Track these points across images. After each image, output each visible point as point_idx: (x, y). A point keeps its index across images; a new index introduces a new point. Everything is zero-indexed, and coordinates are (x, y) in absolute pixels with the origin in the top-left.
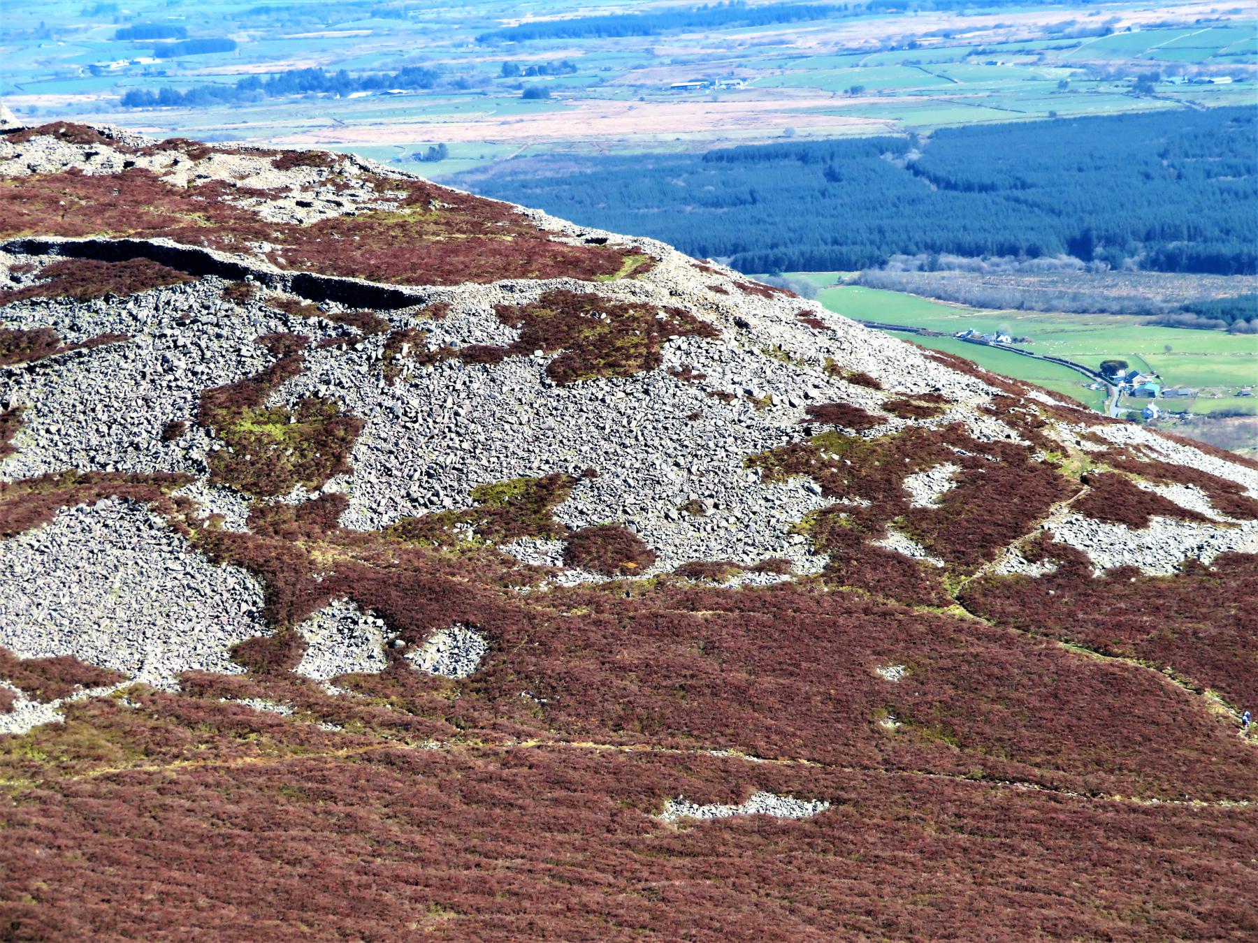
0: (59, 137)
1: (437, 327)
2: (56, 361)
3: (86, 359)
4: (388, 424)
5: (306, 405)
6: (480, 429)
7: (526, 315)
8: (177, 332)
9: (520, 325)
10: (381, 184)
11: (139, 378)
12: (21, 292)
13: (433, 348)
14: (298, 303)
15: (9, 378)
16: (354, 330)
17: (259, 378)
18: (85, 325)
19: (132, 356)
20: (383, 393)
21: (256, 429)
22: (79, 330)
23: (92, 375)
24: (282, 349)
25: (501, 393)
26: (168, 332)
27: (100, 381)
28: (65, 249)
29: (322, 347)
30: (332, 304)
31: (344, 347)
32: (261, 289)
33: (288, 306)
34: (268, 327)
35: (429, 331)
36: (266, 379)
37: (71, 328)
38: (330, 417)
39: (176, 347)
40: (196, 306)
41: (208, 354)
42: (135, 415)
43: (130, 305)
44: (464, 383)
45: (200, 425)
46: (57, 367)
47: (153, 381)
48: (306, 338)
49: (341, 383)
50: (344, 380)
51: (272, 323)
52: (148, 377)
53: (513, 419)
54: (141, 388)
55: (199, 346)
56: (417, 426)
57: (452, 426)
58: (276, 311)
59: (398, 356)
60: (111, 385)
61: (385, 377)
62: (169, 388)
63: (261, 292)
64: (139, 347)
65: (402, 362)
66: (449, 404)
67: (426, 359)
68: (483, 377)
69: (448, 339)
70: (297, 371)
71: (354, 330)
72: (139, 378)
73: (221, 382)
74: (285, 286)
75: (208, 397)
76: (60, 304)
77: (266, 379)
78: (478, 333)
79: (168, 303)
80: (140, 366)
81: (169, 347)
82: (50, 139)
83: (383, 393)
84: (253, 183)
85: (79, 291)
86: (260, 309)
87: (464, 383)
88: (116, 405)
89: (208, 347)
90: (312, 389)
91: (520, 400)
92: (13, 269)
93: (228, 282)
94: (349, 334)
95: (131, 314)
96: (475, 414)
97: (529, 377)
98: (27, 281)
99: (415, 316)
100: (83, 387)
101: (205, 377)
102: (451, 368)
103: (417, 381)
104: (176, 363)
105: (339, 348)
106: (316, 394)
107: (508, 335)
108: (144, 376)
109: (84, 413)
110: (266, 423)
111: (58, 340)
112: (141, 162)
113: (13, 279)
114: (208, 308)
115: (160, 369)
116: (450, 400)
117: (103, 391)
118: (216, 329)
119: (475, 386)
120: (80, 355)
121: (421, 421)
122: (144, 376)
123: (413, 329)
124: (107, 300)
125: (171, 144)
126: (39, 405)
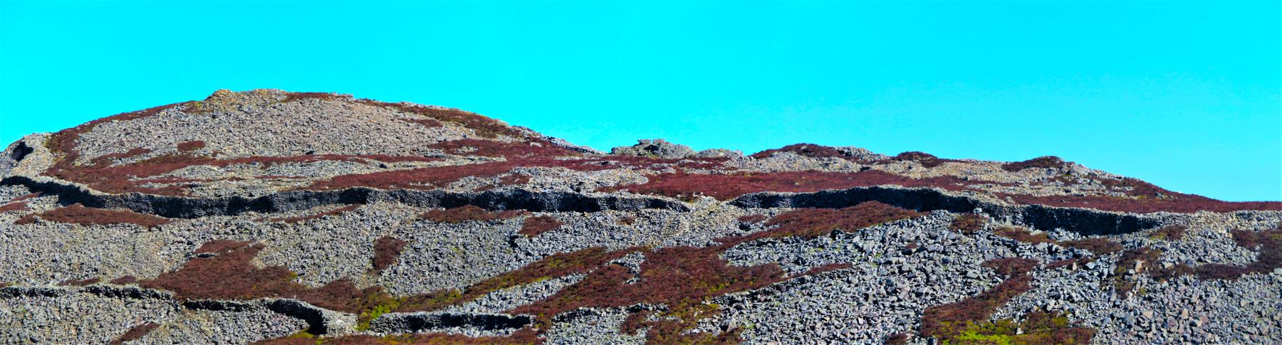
0: (800, 153)
1: (1172, 246)
2: (778, 288)
3: (809, 284)
4: (1120, 334)
5: (1033, 319)
6: (1217, 339)
7: (1264, 238)
8: (902, 260)
9: (1258, 248)
10: (1108, 183)
11: (861, 300)
12: (750, 237)
13: (1167, 265)
14: (1028, 233)
15: (730, 304)
16: (1085, 252)
17: (985, 296)
18: (810, 259)
19: (855, 281)
20: (1114, 306)
21: (981, 338)
22: (804, 263)
23: (814, 299)
24: (1010, 269)
25: (1240, 306)
26: (894, 260)
27: (822, 302)
28: (798, 201)
29: (1052, 267)
30: (1063, 233)
31: (1075, 267)
32: (990, 221)
33: (1017, 235)
34: (996, 254)
35: (1164, 250)
36: (994, 296)
37: (796, 262)
38: (1059, 328)
39: (901, 272)
40: (922, 236)
41: (934, 277)
42: (855, 331)
43: (857, 239)
44: (1201, 297)
45: (922, 336)
46: (779, 294)
47: (875, 302)
48: (1035, 262)
49: (1071, 297)
50: (1074, 295)
51: (1000, 250)
52: (871, 299)
53: (1254, 330)
54: (863, 308)
55: (925, 271)
56: (1150, 335)
57: (1188, 336)
58: (1005, 238)
59: (1131, 271)
60: (833, 306)
61: (1117, 291)
62: (893, 308)
63: (990, 222)
64: (863, 273)
65: (1135, 277)
66: (1185, 315)
67: (1161, 275)
68: (1220, 292)
69: (1183, 257)
70: (1026, 289)
71: (1085, 252)
72: (861, 300)
73: (945, 302)
74: (1014, 217)
75: (931, 313)
76: (787, 242)
77: (994, 296)
78: (1214, 253)
79: (895, 236)
80: (863, 289)
81: (893, 273)
82: (793, 155)
83: (1114, 306)
84: (984, 178)
85: (806, 231)
86: (988, 238)
87: (1201, 297)
88: (836, 323)
89: (933, 272)
90: (1040, 303)
91: (1260, 313)
92: (742, 219)
93: (955, 215)
94: (1080, 256)
95: (857, 246)
96: (1213, 325)
97: (1268, 293)
98: (755, 229)
99: (1151, 235)
100: (804, 309)
101: (929, 298)
102: (1186, 283)
103: (1152, 295)
104: (900, 285)
105: (1070, 267)
106: (1044, 308)
107: (1245, 256)
108: (866, 297)
109: (803, 331)
110: (991, 334)
111: (782, 273)
112: (875, 167)
113: (742, 227)
114: (935, 238)
115: (883, 291)
116: (1185, 311)
117: (824, 311)
118: (943, 256)
119: (1212, 299)
120: (803, 281)
121: (1154, 331)
122: (866, 297)
123: (1147, 248)
124: (833, 237)
125: (907, 156)
126: (758, 325)
